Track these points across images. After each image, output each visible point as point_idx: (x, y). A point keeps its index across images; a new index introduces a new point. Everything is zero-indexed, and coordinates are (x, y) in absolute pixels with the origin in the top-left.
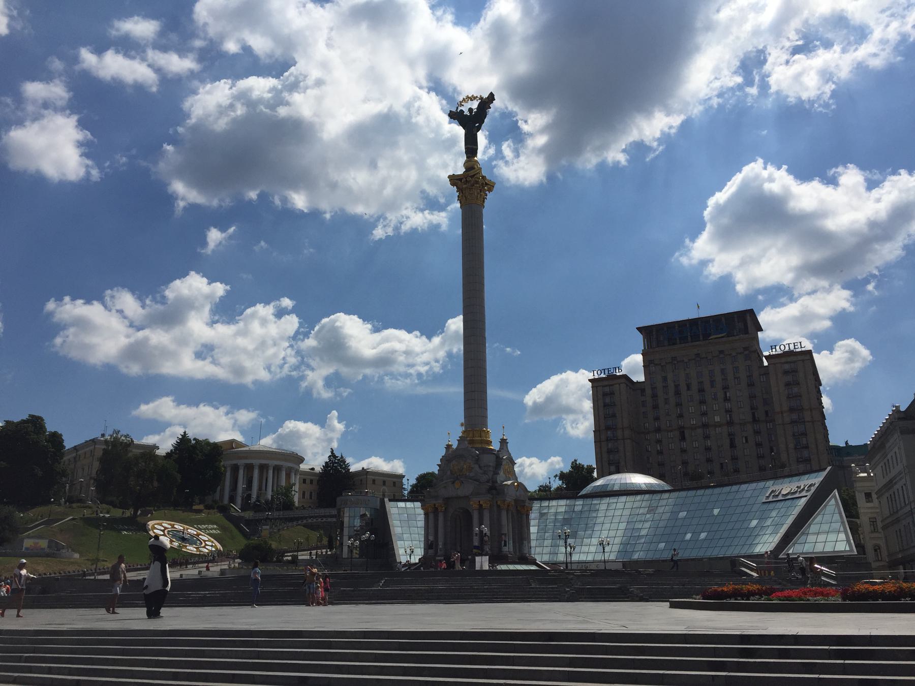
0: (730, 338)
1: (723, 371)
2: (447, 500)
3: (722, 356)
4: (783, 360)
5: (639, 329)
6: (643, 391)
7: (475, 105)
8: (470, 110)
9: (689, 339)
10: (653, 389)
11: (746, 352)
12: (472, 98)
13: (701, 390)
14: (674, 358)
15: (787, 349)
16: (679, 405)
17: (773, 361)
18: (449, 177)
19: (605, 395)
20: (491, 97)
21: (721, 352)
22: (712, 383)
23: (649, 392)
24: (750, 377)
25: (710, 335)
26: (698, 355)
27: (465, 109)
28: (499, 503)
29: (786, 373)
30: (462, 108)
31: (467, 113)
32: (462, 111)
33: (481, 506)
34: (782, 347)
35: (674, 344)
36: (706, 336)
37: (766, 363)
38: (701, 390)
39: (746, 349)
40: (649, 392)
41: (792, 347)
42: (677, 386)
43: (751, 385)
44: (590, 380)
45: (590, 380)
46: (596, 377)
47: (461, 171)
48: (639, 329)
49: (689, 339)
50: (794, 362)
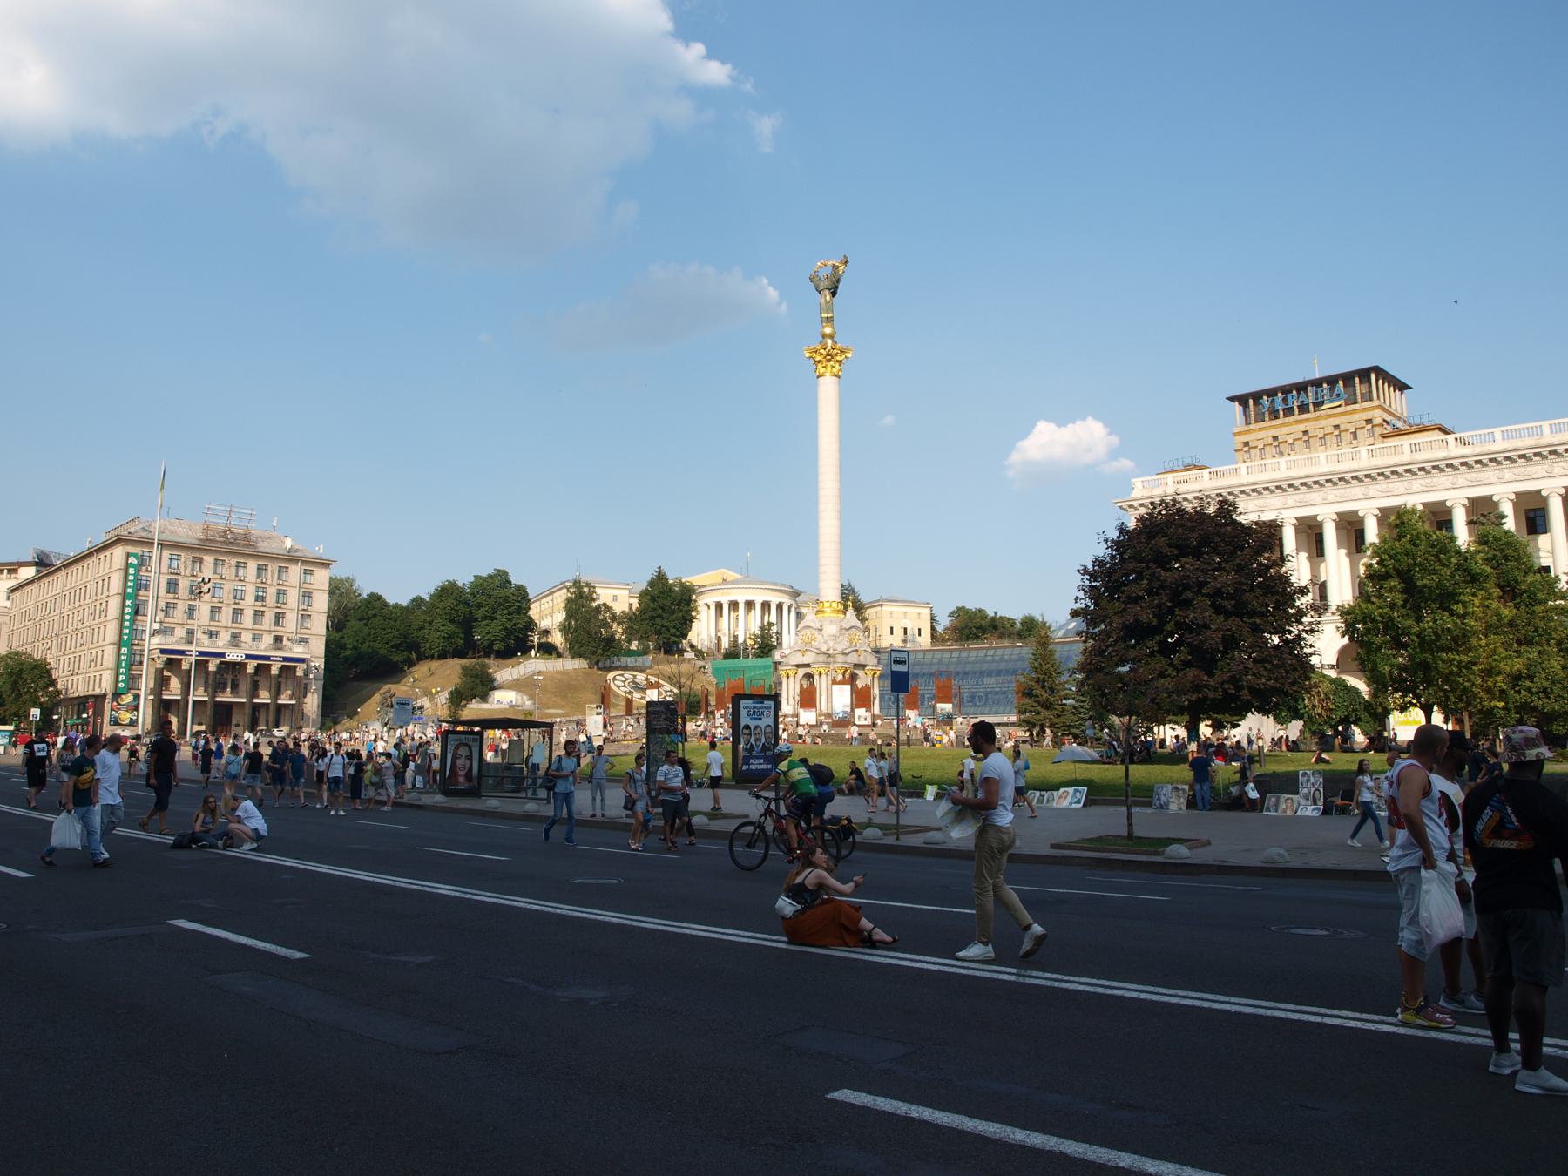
0: (1349, 408)
25: (1322, 403)
36: (1318, 404)
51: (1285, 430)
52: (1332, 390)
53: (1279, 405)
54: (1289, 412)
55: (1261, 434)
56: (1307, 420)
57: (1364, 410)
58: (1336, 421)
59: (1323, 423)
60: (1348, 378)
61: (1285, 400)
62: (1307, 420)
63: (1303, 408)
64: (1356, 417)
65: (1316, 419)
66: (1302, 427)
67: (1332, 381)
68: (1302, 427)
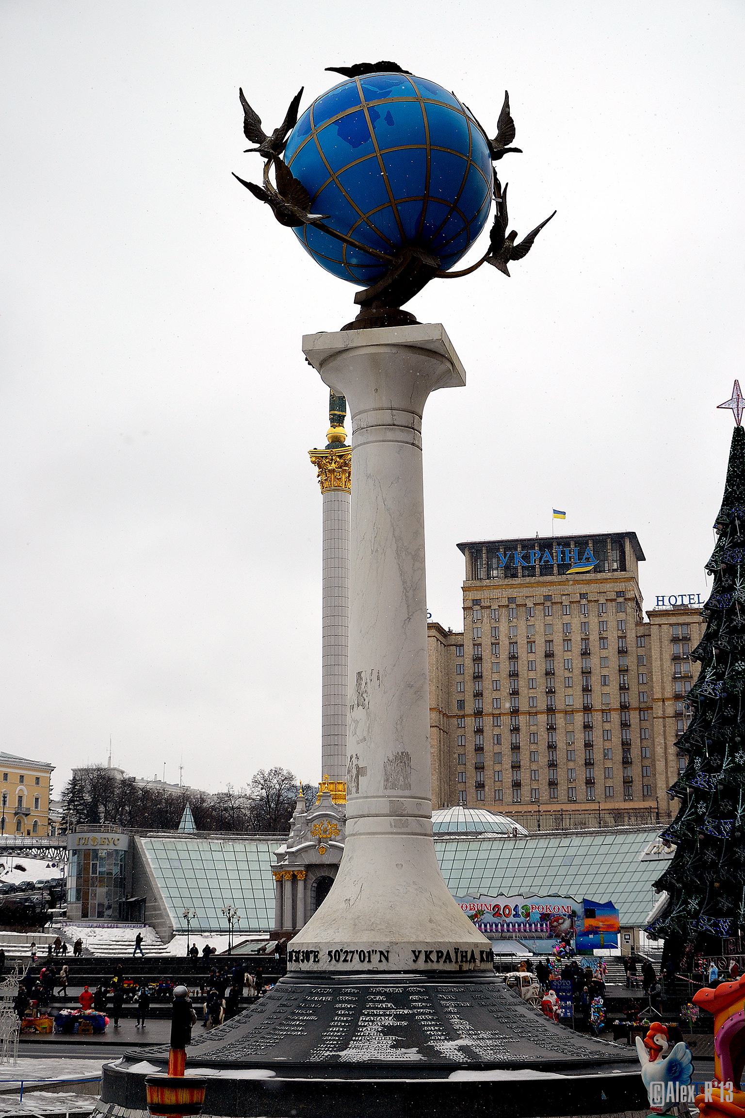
0: (599, 576)
1: (584, 624)
2: (309, 867)
3: (584, 602)
4: (673, 620)
5: (462, 547)
9: (538, 570)
10: (477, 645)
11: (621, 600)
13: (549, 655)
14: (511, 600)
15: (679, 603)
16: (514, 675)
17: (657, 620)
18: (311, 453)
21: (583, 596)
22: (567, 641)
23: (469, 650)
24: (622, 637)
25: (568, 567)
26: (548, 598)
29: (675, 640)
34: (673, 601)
35: (514, 576)
36: (564, 568)
37: (646, 620)
38: (549, 655)
39: (620, 594)
40: (469, 650)
41: (686, 602)
42: (513, 643)
43: (622, 652)
47: (322, 444)
48: (462, 547)
49: (538, 570)
50: (688, 624)
51: (525, 591)
52: (581, 554)
53: (519, 562)
54: (530, 571)
55: (496, 593)
56: (552, 583)
57: (616, 580)
58: (584, 589)
59: (569, 589)
60: (600, 540)
61: (526, 558)
62: (552, 583)
63: (546, 570)
64: (608, 587)
65: (560, 583)
66: (545, 591)
67: (581, 542)
68: (545, 591)
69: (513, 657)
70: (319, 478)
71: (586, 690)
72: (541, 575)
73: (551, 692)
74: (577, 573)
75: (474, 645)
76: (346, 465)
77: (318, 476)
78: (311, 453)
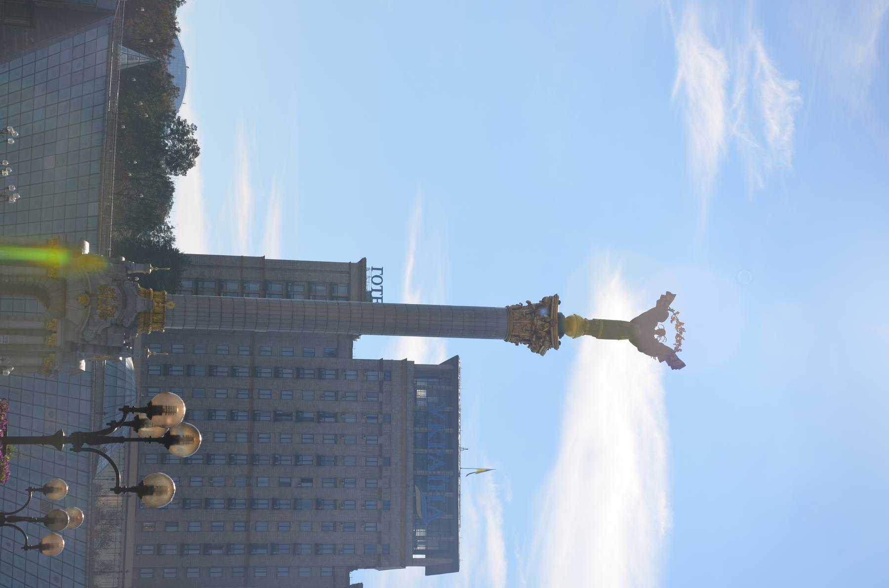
6: (333, 354)
7: (669, 341)
8: (662, 332)
12: (679, 338)
18: (556, 296)
19: (332, 286)
20: (676, 364)
26: (388, 462)
27: (667, 325)
28: (53, 355)
30: (669, 319)
31: (660, 326)
32: (663, 318)
33: (51, 332)
35: (416, 423)
43: (317, 548)
44: (364, 261)
45: (364, 261)
46: (368, 273)
69: (320, 416)
70: (525, 304)
71: (274, 503)
72: (415, 455)
73: (275, 460)
74: (415, 498)
75: (337, 371)
76: (538, 338)
77: (528, 302)
78: (556, 296)
